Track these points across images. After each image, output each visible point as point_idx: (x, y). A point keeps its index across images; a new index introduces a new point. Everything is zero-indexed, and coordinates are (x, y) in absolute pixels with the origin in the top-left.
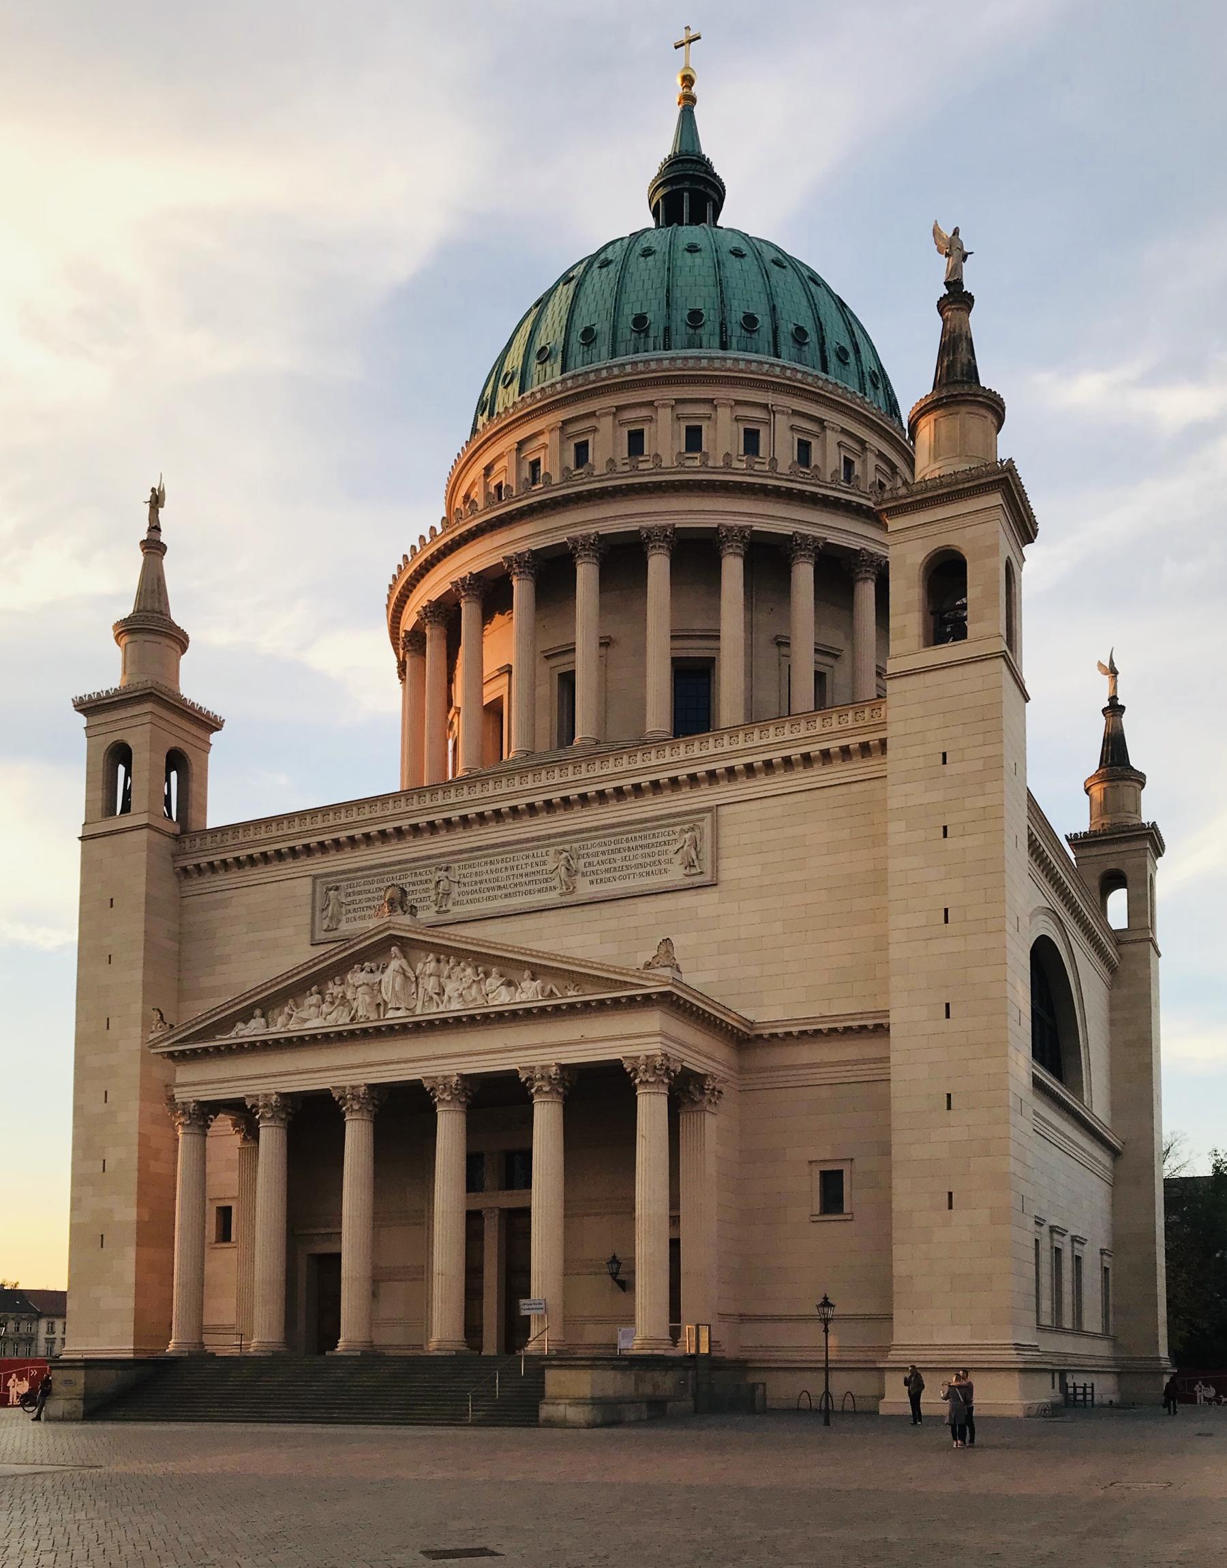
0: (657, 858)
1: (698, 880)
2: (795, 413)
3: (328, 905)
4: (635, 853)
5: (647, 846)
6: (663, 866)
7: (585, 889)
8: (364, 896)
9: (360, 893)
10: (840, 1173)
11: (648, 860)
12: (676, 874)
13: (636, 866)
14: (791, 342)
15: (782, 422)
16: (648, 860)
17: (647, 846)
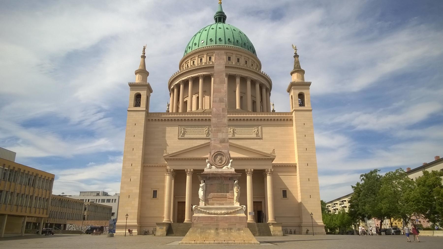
0: (250, 132)
1: (258, 137)
2: (252, 60)
3: (182, 131)
4: (246, 130)
5: (248, 130)
6: (251, 134)
7: (237, 136)
8: (190, 131)
9: (188, 130)
10: (286, 190)
11: (249, 132)
12: (254, 136)
13: (247, 133)
14: (250, 48)
15: (250, 61)
16: (249, 132)
17: (248, 130)
